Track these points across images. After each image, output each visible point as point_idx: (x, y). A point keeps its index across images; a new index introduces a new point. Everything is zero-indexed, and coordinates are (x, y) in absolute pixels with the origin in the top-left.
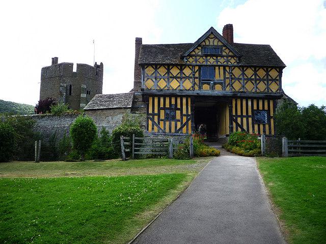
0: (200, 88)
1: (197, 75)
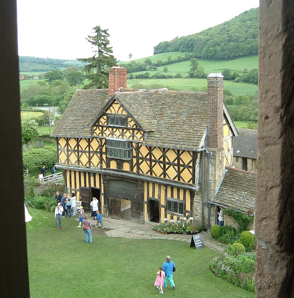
1: (104, 150)
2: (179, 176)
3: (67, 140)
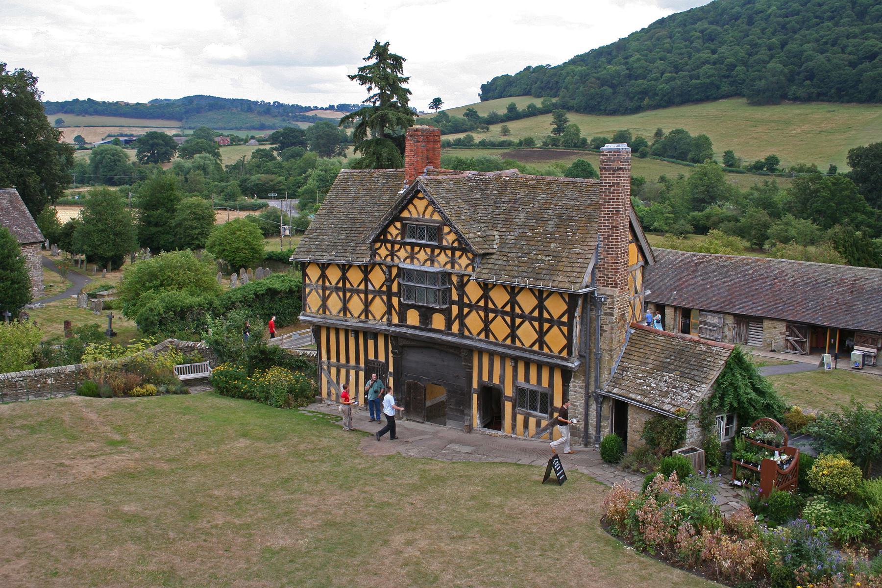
1: (395, 288)
2: (541, 341)
3: (324, 267)
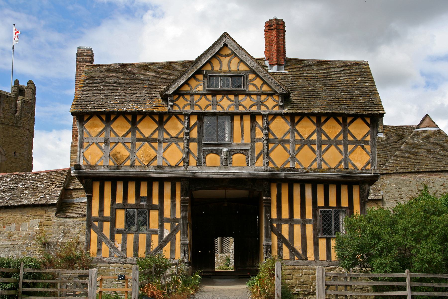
0: (200, 162)
